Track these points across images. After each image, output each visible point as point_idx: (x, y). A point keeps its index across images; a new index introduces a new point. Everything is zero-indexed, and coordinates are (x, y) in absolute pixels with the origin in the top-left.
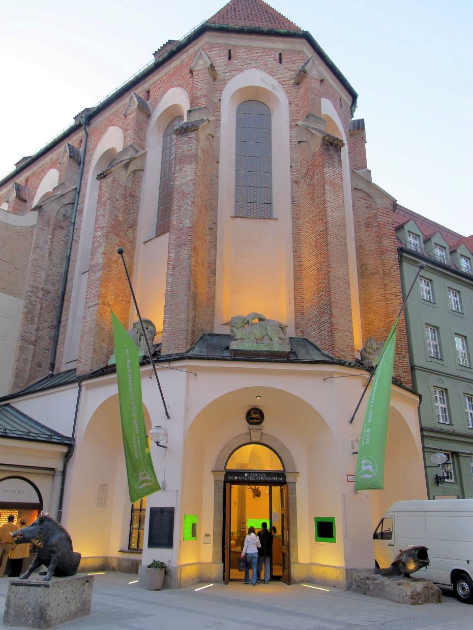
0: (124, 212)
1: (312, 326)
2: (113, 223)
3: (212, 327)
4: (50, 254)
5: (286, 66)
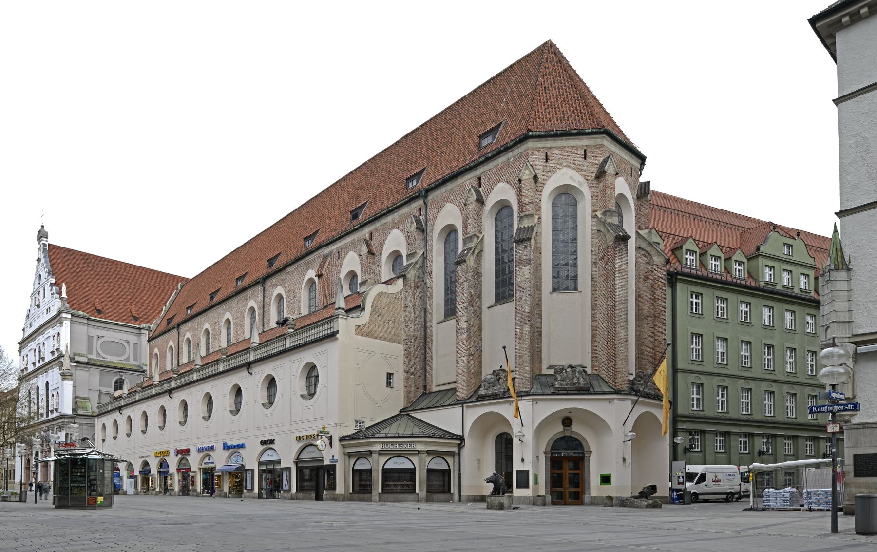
3: (541, 370)
4: (414, 308)
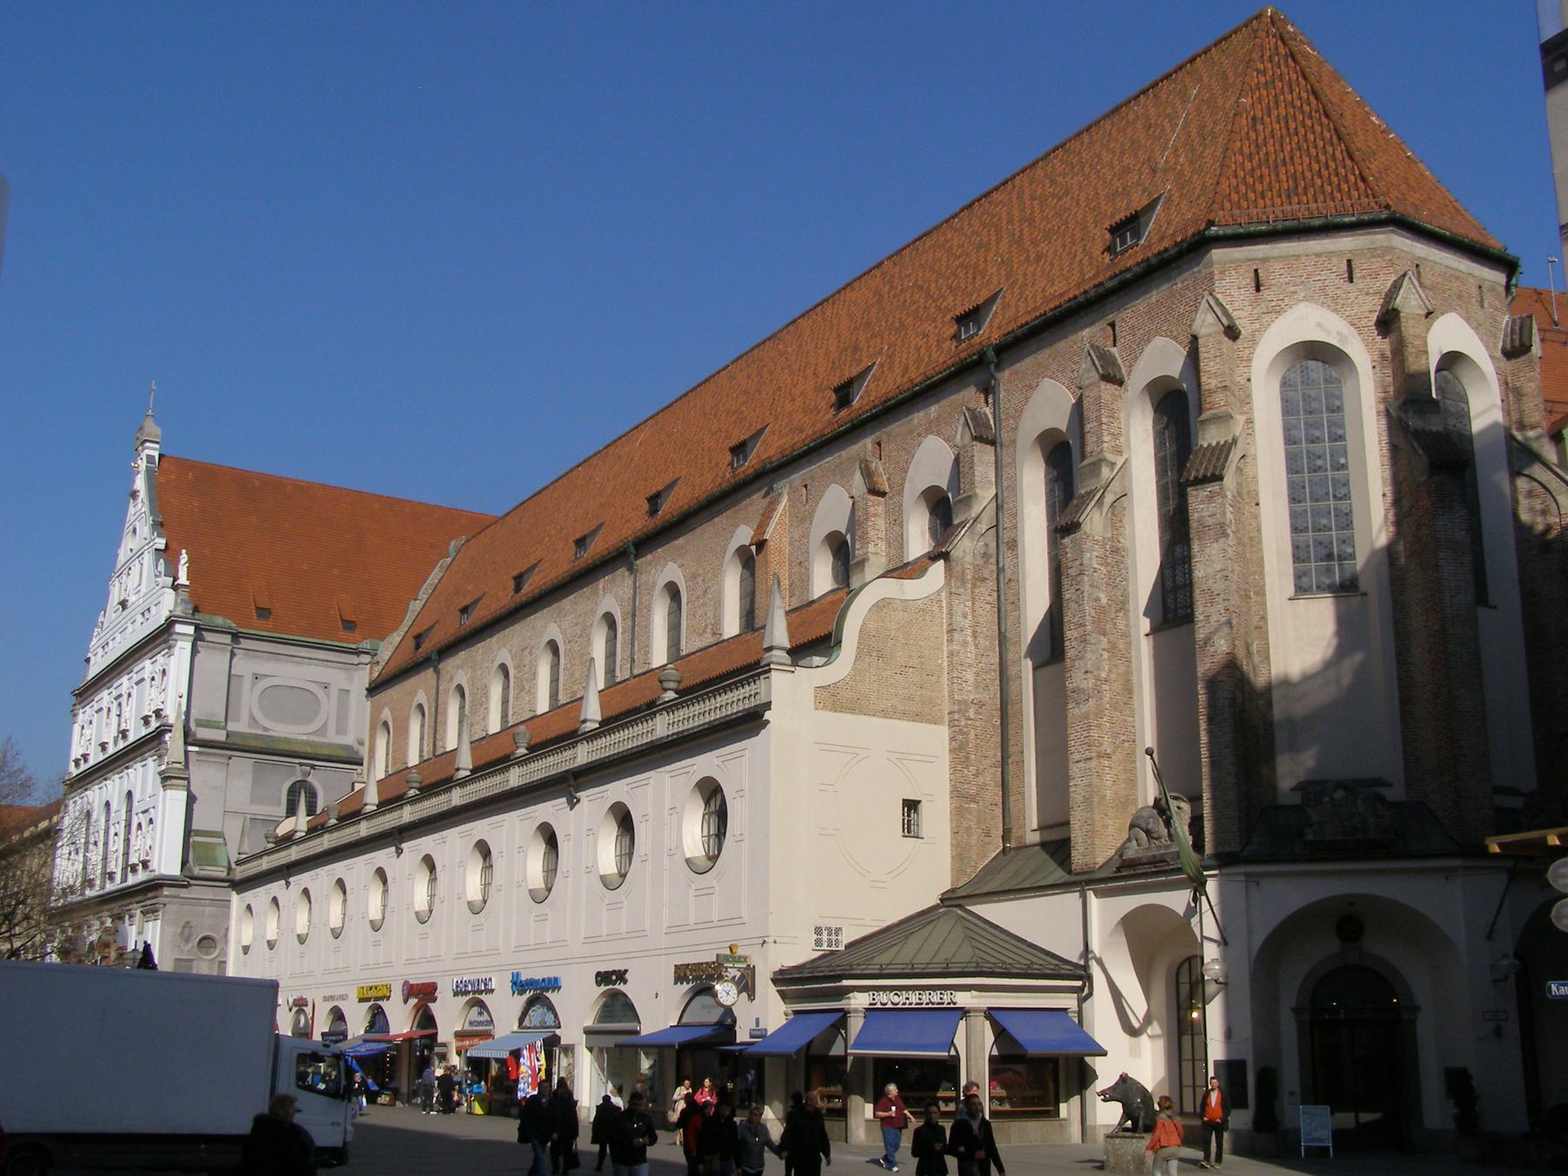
5: (1362, 286)
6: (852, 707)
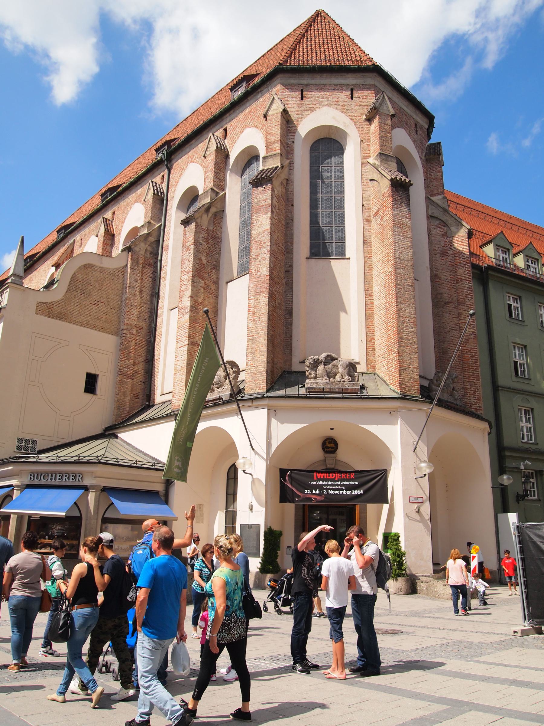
0: (207, 254)
1: (381, 362)
2: (198, 267)
3: (290, 365)
4: (141, 292)
5: (358, 102)
6: (60, 317)
